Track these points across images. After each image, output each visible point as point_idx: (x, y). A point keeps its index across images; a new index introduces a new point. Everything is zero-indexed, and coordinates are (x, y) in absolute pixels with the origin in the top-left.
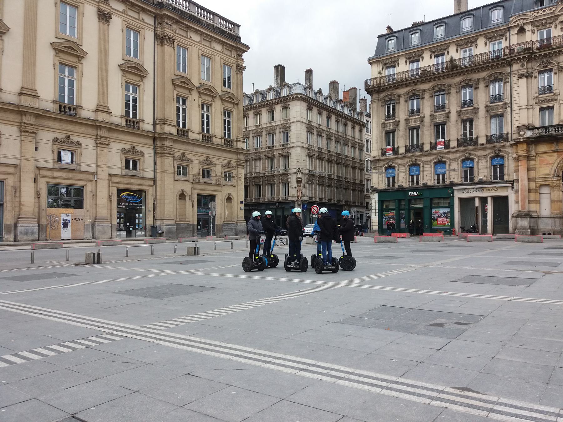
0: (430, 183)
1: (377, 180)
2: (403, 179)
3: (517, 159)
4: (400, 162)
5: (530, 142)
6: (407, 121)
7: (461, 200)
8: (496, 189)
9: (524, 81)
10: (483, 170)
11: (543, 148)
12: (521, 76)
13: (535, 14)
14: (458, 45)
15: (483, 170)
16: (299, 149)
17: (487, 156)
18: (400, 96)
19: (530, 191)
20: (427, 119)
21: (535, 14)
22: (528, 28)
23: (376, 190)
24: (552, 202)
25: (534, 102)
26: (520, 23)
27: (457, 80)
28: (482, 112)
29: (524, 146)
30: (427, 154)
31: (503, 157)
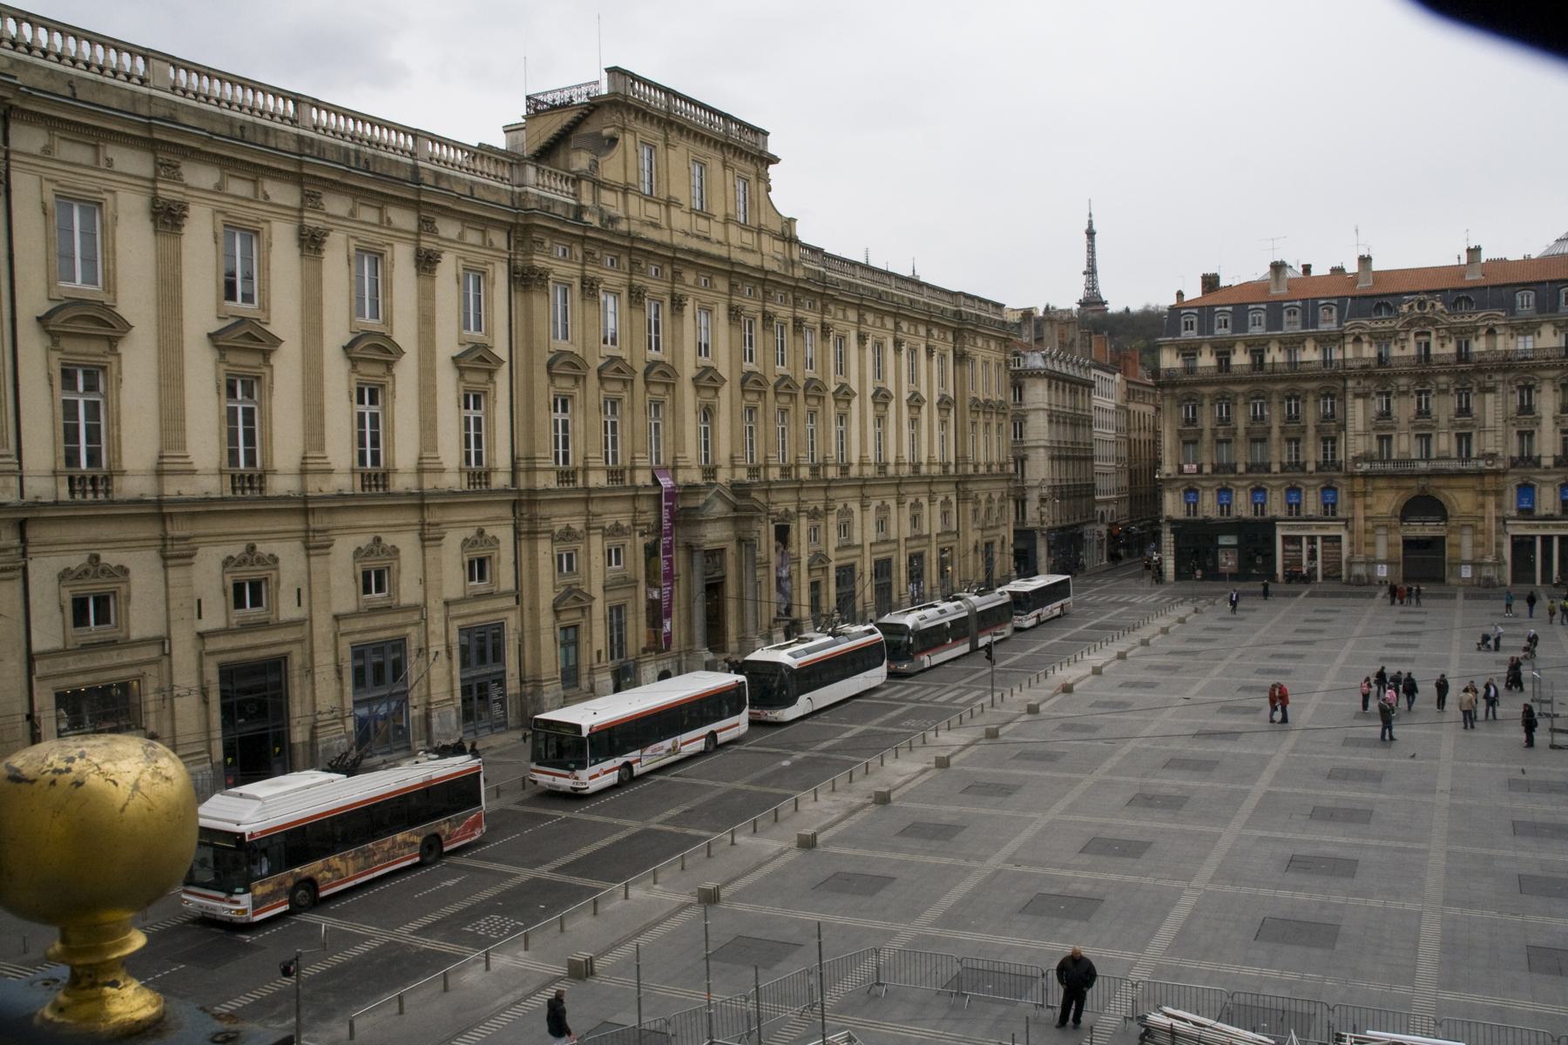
0: (1244, 515)
1: (1172, 505)
2: (1209, 506)
3: (1353, 495)
4: (1205, 484)
5: (1366, 476)
6: (1214, 432)
7: (1284, 538)
8: (1327, 527)
9: (1360, 402)
10: (1312, 503)
11: (1381, 483)
12: (1357, 396)
13: (1373, 325)
14: (1281, 342)
15: (1312, 503)
16: (1042, 451)
17: (1315, 486)
18: (1203, 395)
19: (1366, 531)
20: (1241, 432)
21: (1373, 325)
22: (1365, 338)
23: (1171, 521)
24: (1389, 545)
25: (1371, 427)
26: (1357, 331)
27: (1280, 387)
28: (1311, 432)
29: (1361, 481)
30: (1241, 477)
31: (1335, 490)
